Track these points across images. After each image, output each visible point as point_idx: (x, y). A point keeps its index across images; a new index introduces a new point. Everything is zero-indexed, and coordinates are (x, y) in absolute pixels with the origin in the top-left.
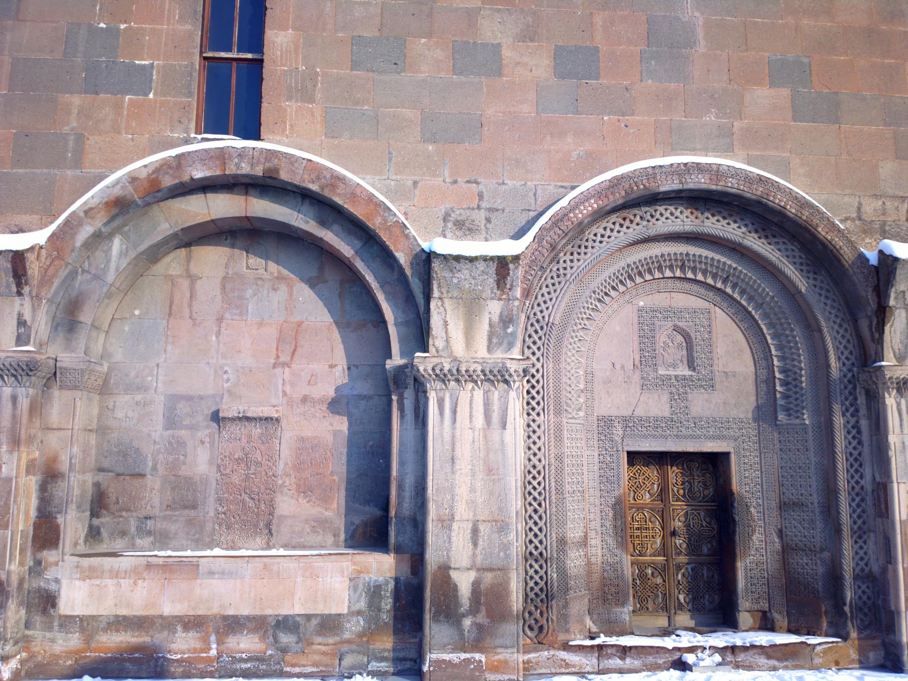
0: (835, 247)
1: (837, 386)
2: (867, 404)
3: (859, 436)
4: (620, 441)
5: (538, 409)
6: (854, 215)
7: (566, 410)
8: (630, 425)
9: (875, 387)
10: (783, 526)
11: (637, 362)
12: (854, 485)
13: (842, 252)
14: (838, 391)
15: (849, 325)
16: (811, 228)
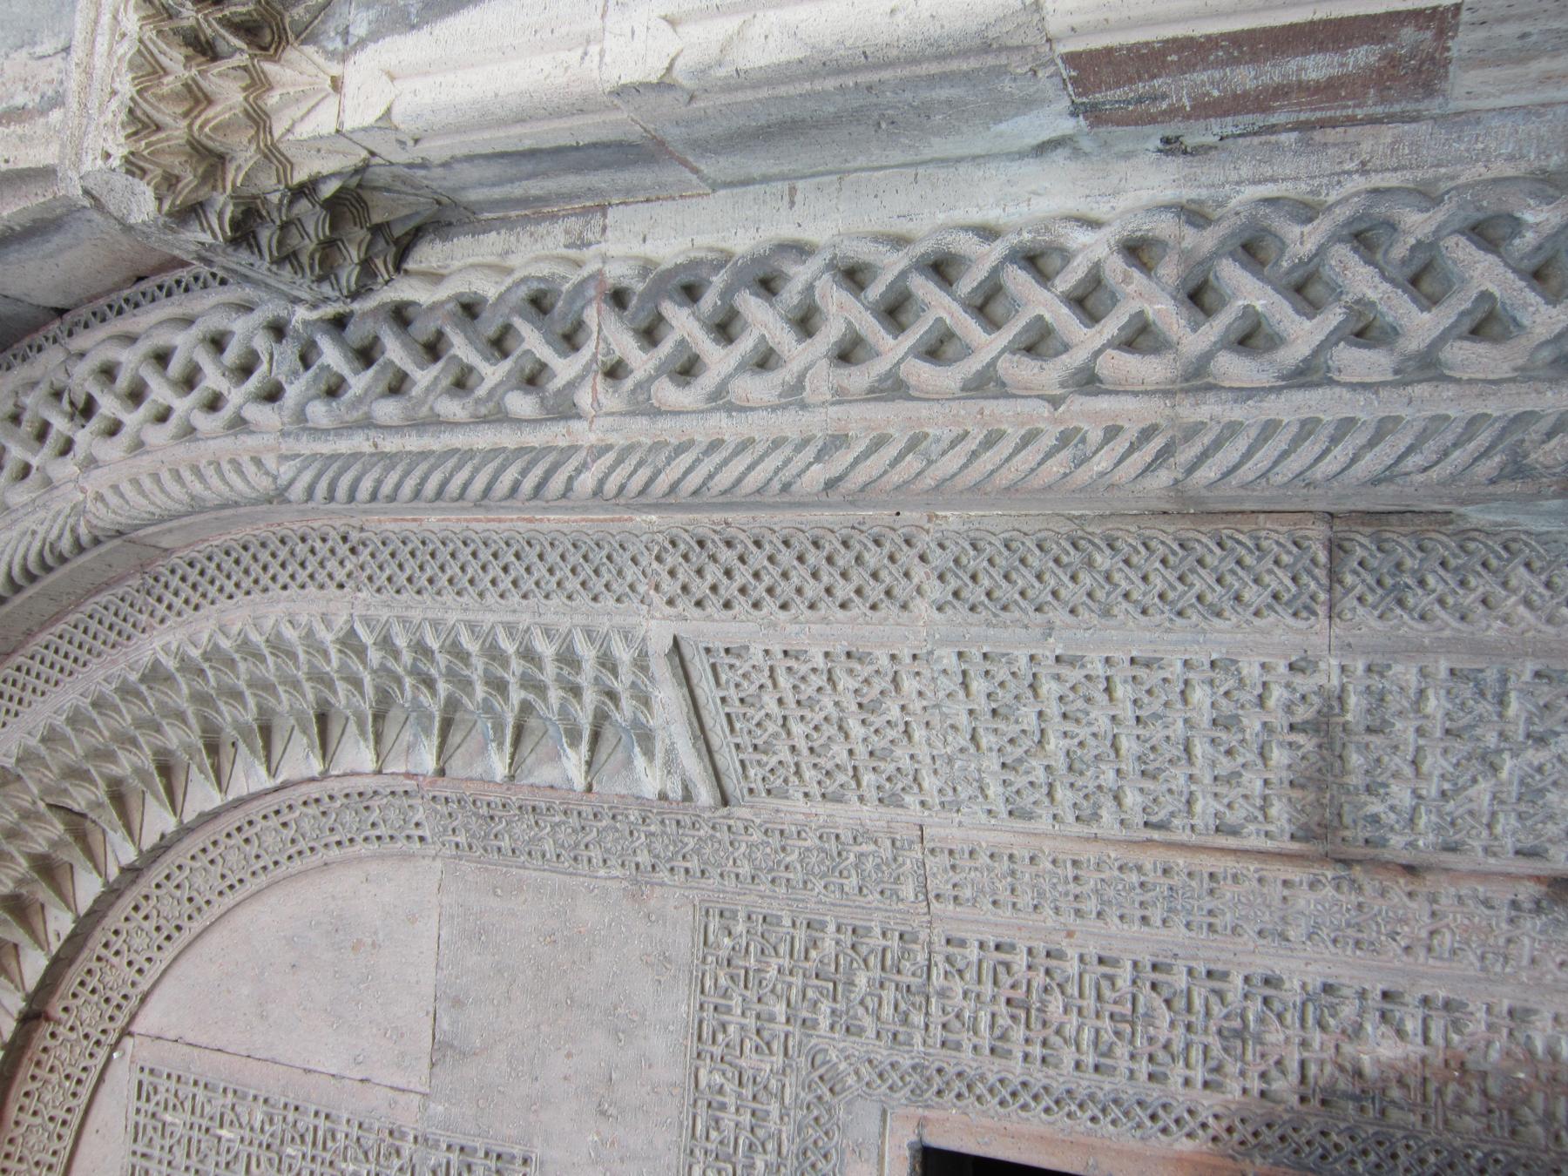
1: (391, 444)
2: (506, 224)
3: (718, 280)
12: (1111, 326)
14: (413, 443)
15: (82, 355)
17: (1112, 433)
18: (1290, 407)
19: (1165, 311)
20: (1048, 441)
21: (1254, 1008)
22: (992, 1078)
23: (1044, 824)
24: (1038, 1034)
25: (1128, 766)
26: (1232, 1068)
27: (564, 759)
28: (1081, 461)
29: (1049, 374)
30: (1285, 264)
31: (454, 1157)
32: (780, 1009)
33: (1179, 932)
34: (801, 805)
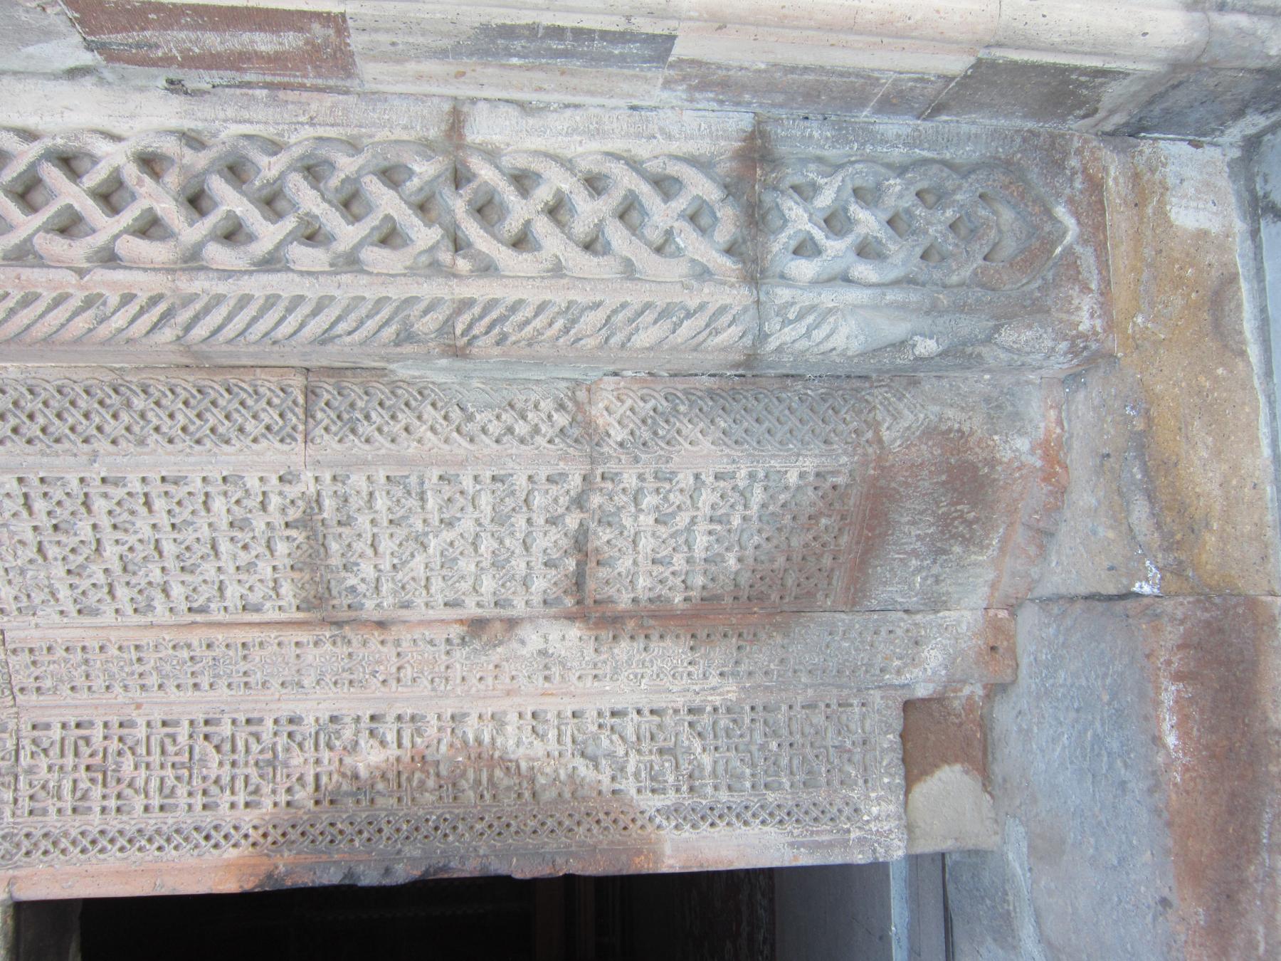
12: (128, 217)
17: (127, 299)
18: (260, 285)
19: (169, 210)
20: (75, 303)
21: (282, 740)
22: (74, 833)
23: (108, 617)
24: (113, 789)
25: (171, 564)
26: (266, 789)
28: (101, 320)
29: (78, 250)
30: (257, 183)
33: (223, 692)
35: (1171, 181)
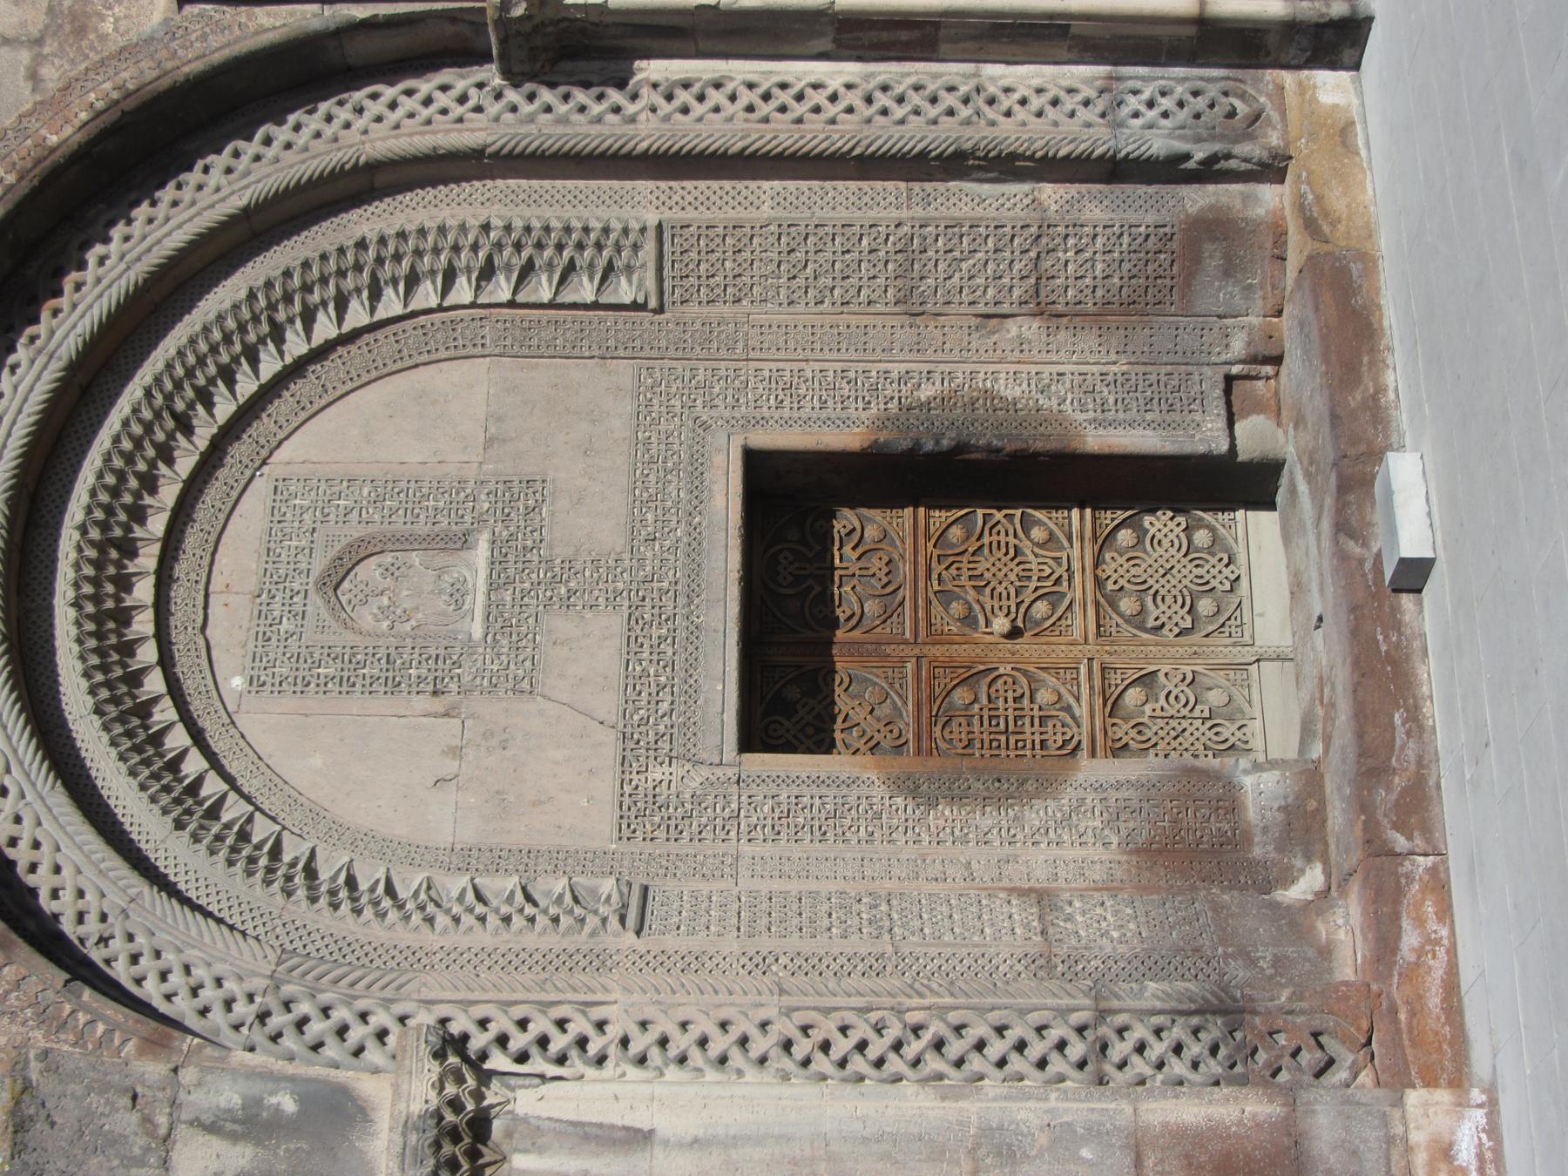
0: (117, 102)
4: (705, 771)
5: (578, 1026)
6: (25, 56)
7: (593, 934)
8: (652, 738)
9: (550, 29)
10: (972, 310)
11: (438, 704)
13: (131, 86)
16: (47, 163)
27: (582, 292)
31: (500, 486)
32: (678, 403)
34: (696, 309)
35: (1319, 84)
